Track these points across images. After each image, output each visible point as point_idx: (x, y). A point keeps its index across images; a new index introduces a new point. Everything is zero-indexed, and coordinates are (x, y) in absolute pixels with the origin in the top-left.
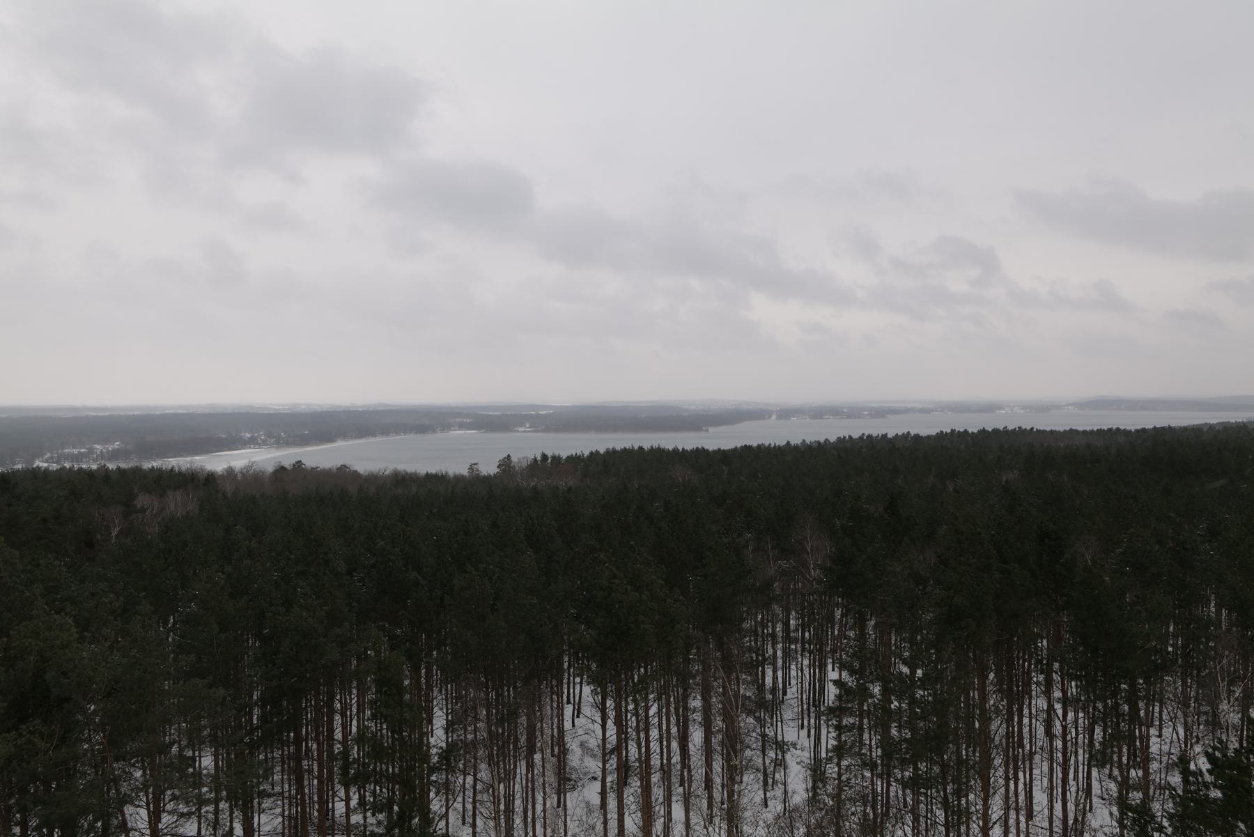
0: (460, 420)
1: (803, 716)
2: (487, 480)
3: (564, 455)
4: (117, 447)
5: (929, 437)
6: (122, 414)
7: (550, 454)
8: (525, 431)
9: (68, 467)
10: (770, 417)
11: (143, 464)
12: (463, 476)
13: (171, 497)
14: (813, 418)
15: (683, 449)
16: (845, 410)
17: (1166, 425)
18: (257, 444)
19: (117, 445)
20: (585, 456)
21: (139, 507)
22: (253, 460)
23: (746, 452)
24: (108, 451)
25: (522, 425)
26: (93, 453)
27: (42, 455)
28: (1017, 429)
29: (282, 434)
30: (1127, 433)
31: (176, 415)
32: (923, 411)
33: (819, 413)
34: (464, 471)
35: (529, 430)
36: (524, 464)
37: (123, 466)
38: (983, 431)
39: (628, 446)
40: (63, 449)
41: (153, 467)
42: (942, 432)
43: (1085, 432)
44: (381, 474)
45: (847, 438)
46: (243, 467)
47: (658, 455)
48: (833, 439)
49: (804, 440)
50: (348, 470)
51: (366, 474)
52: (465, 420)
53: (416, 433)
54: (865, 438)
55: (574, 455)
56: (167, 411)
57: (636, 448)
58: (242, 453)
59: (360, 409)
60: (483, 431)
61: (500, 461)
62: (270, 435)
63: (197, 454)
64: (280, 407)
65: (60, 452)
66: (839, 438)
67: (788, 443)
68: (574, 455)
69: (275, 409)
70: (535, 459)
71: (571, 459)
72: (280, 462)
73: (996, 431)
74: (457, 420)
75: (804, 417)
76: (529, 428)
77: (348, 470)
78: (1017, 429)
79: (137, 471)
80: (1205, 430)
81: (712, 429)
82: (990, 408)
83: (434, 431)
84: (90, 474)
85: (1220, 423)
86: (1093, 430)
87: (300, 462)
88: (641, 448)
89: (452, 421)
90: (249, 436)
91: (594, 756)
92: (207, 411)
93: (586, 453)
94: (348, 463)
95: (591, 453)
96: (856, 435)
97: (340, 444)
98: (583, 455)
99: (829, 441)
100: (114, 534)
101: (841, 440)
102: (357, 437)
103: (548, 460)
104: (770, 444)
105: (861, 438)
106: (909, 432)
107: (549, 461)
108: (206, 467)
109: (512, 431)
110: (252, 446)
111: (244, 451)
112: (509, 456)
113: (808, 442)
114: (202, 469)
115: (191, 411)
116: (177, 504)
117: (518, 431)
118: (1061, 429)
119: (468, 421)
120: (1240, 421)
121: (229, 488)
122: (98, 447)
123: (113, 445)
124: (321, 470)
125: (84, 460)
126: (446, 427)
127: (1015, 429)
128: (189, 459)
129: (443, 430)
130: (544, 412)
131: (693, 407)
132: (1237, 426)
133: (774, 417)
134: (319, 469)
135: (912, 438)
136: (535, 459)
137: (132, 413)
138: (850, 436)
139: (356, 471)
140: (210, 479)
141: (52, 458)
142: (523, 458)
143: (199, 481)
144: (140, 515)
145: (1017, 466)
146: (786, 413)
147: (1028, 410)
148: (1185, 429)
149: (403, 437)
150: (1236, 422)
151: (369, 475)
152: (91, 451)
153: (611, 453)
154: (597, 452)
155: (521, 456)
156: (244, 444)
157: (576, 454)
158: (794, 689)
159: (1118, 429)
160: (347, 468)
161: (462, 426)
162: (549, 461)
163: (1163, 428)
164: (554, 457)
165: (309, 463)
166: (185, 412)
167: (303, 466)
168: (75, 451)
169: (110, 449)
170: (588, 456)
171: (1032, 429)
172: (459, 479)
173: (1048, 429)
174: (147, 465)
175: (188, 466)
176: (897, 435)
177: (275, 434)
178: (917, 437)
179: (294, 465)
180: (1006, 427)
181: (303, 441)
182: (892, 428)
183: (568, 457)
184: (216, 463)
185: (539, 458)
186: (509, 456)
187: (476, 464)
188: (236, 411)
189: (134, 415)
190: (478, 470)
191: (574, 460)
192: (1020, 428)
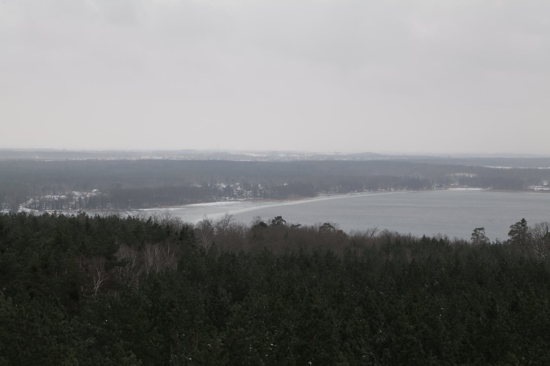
8: (542, 191)
9: (50, 213)
11: (120, 213)
12: (466, 243)
13: (148, 251)
19: (95, 192)
21: (119, 260)
22: (231, 212)
25: (537, 183)
27: (26, 200)
35: (547, 189)
37: (102, 215)
40: (45, 194)
41: (129, 217)
44: (369, 235)
46: (220, 220)
50: (332, 229)
51: (353, 235)
52: (467, 175)
60: (489, 189)
65: (42, 197)
76: (546, 186)
77: (332, 229)
79: (115, 220)
83: (430, 188)
84: (73, 221)
87: (279, 218)
89: (452, 175)
90: (224, 186)
94: (332, 221)
97: (322, 199)
100: (97, 288)
108: (182, 219)
109: (526, 190)
111: (218, 203)
121: (206, 244)
122: (77, 193)
124: (302, 229)
125: (64, 207)
126: (444, 183)
128: (163, 210)
129: (440, 187)
134: (300, 227)
139: (341, 231)
141: (34, 203)
143: (176, 233)
149: (392, 193)
151: (355, 236)
152: (70, 197)
160: (332, 227)
161: (463, 182)
165: (290, 220)
167: (284, 223)
168: (56, 197)
169: (88, 196)
174: (125, 215)
175: (165, 217)
179: (273, 221)
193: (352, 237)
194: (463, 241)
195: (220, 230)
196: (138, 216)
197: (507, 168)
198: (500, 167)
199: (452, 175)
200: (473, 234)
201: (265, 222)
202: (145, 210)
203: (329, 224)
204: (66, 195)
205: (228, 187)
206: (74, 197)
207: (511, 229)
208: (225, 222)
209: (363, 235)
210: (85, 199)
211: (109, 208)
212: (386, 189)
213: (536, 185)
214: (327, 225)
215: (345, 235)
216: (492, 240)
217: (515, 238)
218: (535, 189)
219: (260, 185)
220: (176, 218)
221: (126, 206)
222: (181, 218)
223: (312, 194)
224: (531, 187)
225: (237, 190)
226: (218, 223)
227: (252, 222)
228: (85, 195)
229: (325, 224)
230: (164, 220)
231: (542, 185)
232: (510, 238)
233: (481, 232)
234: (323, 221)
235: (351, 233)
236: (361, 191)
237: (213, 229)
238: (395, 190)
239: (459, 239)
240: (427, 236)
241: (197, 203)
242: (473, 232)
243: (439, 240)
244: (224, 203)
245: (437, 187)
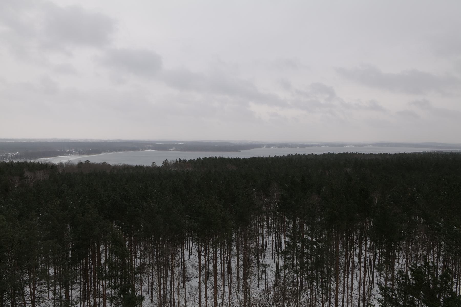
0: (149, 146)
1: (272, 255)
2: (159, 168)
3: (187, 160)
4: (17, 154)
5: (320, 155)
6: (19, 141)
7: (182, 159)
10: (263, 147)
11: (27, 160)
14: (279, 147)
15: (231, 158)
16: (290, 145)
17: (404, 152)
19: (18, 153)
20: (195, 160)
22: (70, 160)
23: (254, 160)
28: (351, 153)
29: (81, 150)
30: (390, 155)
31: (40, 142)
32: (318, 146)
33: (281, 146)
34: (150, 165)
36: (172, 163)
37: (20, 161)
38: (340, 153)
39: (211, 156)
42: (325, 153)
43: (375, 154)
44: (119, 165)
45: (291, 155)
47: (222, 160)
48: (286, 155)
49: (275, 156)
50: (106, 164)
52: (150, 146)
53: (132, 150)
54: (297, 155)
55: (191, 160)
56: (37, 141)
57: (214, 157)
59: (111, 141)
61: (163, 161)
62: (76, 150)
63: (48, 157)
66: (288, 155)
67: (270, 156)
68: (191, 160)
70: (177, 161)
72: (80, 161)
73: (344, 154)
74: (148, 146)
75: (275, 147)
76: (174, 149)
77: (106, 164)
78: (351, 153)
80: (417, 154)
81: (242, 151)
82: (342, 145)
83: (139, 150)
84: (7, 164)
85: (422, 152)
86: (378, 154)
88: (216, 157)
90: (68, 150)
91: (196, 269)
92: (52, 141)
93: (196, 159)
94: (106, 161)
95: (198, 159)
96: (294, 154)
97: (103, 154)
99: (284, 156)
100: (16, 186)
101: (289, 156)
102: (110, 152)
103: (181, 161)
104: (263, 157)
105: (296, 155)
106: (313, 153)
107: (182, 162)
111: (66, 156)
112: (167, 159)
113: (277, 156)
114: (50, 163)
115: (46, 141)
116: (41, 175)
118: (366, 153)
120: (429, 151)
121: (61, 170)
122: (10, 154)
124: (96, 164)
125: (4, 159)
126: (143, 148)
127: (351, 153)
128: (45, 159)
130: (180, 144)
131: (235, 143)
132: (428, 153)
133: (265, 147)
134: (95, 163)
135: (314, 155)
136: (177, 161)
137: (23, 142)
138: (292, 154)
139: (109, 164)
140: (54, 167)
142: (172, 160)
143: (49, 167)
144: (26, 179)
145: (351, 166)
146: (269, 146)
147: (355, 146)
148: (410, 154)
149: (127, 152)
150: (428, 152)
152: (7, 155)
153: (205, 159)
154: (200, 159)
155: (171, 160)
156: (67, 154)
158: (270, 245)
159: (387, 154)
161: (149, 148)
162: (182, 162)
163: (403, 154)
164: (183, 160)
165: (91, 161)
166: (44, 141)
169: (15, 155)
170: (196, 160)
171: (357, 153)
172: (148, 168)
173: (362, 153)
174: (28, 161)
176: (309, 154)
177: (79, 150)
178: (316, 155)
179: (86, 162)
180: (347, 152)
181: (89, 153)
182: (307, 152)
184: (56, 161)
185: (178, 161)
186: (167, 159)
187: (155, 162)
190: (155, 165)
192: (352, 152)
194: (148, 166)
196: (35, 161)
198: (160, 144)
201: (82, 162)
203: (105, 162)
206: (9, 155)
208: (68, 162)
210: (13, 156)
213: (171, 149)
214: (105, 163)
215: (110, 165)
221: (30, 157)
223: (99, 152)
226: (66, 163)
227: (78, 162)
229: (104, 162)
230: (45, 162)
231: (173, 149)
234: (103, 162)
235: (113, 165)
237: (64, 165)
239: (148, 166)
243: (141, 166)
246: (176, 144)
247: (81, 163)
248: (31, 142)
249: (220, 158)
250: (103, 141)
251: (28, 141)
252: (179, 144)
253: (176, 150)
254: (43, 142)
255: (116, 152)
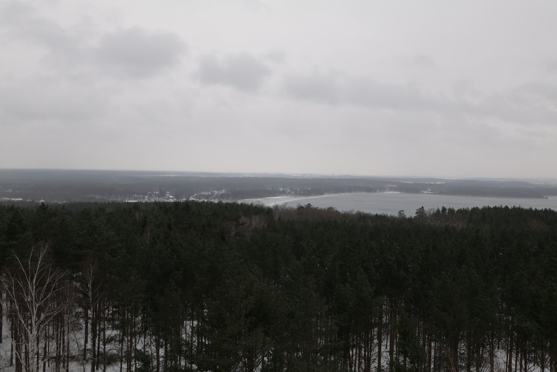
0: (390, 185)
2: (410, 219)
4: (223, 192)
6: (226, 176)
15: (536, 209)
18: (286, 194)
20: (470, 210)
22: (287, 201)
24: (220, 194)
26: (213, 195)
27: (193, 194)
29: (298, 189)
31: (249, 178)
34: (396, 214)
35: (430, 193)
40: (202, 192)
47: (518, 212)
51: (343, 213)
52: (393, 186)
55: (462, 209)
56: (245, 176)
58: (279, 198)
59: (336, 178)
62: (292, 190)
63: (258, 197)
64: (297, 176)
65: (200, 193)
68: (462, 209)
69: (295, 177)
70: (438, 210)
71: (460, 211)
72: (300, 204)
74: (388, 185)
76: (430, 191)
83: (376, 192)
87: (309, 204)
89: (386, 186)
90: (282, 189)
92: (263, 176)
98: (468, 209)
102: (335, 193)
103: (446, 210)
107: (447, 211)
109: (420, 193)
110: (283, 195)
112: (423, 207)
115: (256, 176)
117: (424, 193)
119: (395, 186)
122: (216, 192)
123: (222, 191)
125: (210, 198)
126: (382, 189)
130: (439, 183)
134: (318, 208)
136: (438, 210)
137: (230, 177)
139: (337, 211)
141: (197, 196)
142: (432, 209)
149: (359, 193)
151: (345, 213)
152: (213, 194)
153: (487, 210)
154: (477, 208)
155: (430, 208)
157: (464, 208)
160: (333, 209)
161: (391, 189)
162: (447, 211)
165: (314, 205)
166: (253, 176)
167: (311, 207)
168: (206, 194)
169: (221, 193)
172: (393, 219)
175: (257, 203)
179: (307, 206)
181: (308, 193)
183: (459, 210)
184: (270, 202)
185: (441, 210)
186: (423, 207)
187: (403, 211)
188: (276, 177)
189: (231, 177)
190: (403, 214)
191: (463, 212)
193: (343, 214)
195: (283, 209)
196: (245, 202)
197: (412, 183)
198: (408, 182)
199: (386, 186)
200: (398, 213)
202: (246, 200)
203: (331, 207)
204: (211, 193)
205: (284, 190)
206: (215, 194)
207: (416, 211)
209: (348, 213)
211: (230, 199)
212: (355, 191)
213: (425, 191)
214: (331, 208)
216: (408, 216)
217: (419, 215)
218: (425, 192)
219: (298, 189)
220: (262, 204)
222: (264, 204)
224: (423, 192)
225: (288, 191)
226: (281, 206)
228: (219, 193)
229: (330, 207)
230: (257, 204)
231: (428, 191)
232: (416, 215)
233: (402, 212)
235: (342, 211)
236: (344, 193)
237: (279, 209)
238: (360, 192)
240: (378, 214)
241: (270, 197)
242: (399, 212)
244: (282, 197)
245: (379, 191)
246: (433, 183)
247: (302, 207)
248: (239, 177)
249: (514, 209)
250: (326, 178)
251: (236, 176)
252: (437, 183)
253: (432, 192)
254: (252, 177)
255: (343, 192)
